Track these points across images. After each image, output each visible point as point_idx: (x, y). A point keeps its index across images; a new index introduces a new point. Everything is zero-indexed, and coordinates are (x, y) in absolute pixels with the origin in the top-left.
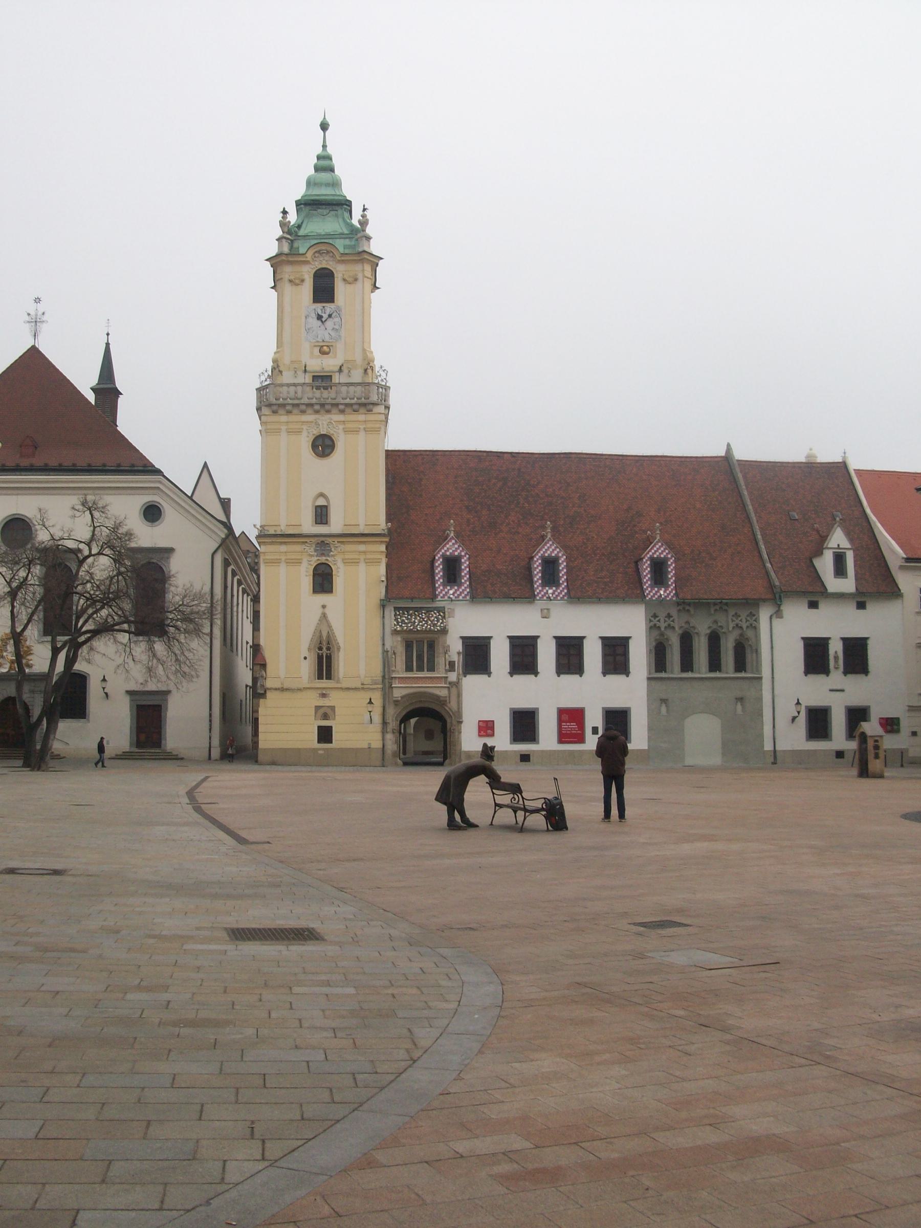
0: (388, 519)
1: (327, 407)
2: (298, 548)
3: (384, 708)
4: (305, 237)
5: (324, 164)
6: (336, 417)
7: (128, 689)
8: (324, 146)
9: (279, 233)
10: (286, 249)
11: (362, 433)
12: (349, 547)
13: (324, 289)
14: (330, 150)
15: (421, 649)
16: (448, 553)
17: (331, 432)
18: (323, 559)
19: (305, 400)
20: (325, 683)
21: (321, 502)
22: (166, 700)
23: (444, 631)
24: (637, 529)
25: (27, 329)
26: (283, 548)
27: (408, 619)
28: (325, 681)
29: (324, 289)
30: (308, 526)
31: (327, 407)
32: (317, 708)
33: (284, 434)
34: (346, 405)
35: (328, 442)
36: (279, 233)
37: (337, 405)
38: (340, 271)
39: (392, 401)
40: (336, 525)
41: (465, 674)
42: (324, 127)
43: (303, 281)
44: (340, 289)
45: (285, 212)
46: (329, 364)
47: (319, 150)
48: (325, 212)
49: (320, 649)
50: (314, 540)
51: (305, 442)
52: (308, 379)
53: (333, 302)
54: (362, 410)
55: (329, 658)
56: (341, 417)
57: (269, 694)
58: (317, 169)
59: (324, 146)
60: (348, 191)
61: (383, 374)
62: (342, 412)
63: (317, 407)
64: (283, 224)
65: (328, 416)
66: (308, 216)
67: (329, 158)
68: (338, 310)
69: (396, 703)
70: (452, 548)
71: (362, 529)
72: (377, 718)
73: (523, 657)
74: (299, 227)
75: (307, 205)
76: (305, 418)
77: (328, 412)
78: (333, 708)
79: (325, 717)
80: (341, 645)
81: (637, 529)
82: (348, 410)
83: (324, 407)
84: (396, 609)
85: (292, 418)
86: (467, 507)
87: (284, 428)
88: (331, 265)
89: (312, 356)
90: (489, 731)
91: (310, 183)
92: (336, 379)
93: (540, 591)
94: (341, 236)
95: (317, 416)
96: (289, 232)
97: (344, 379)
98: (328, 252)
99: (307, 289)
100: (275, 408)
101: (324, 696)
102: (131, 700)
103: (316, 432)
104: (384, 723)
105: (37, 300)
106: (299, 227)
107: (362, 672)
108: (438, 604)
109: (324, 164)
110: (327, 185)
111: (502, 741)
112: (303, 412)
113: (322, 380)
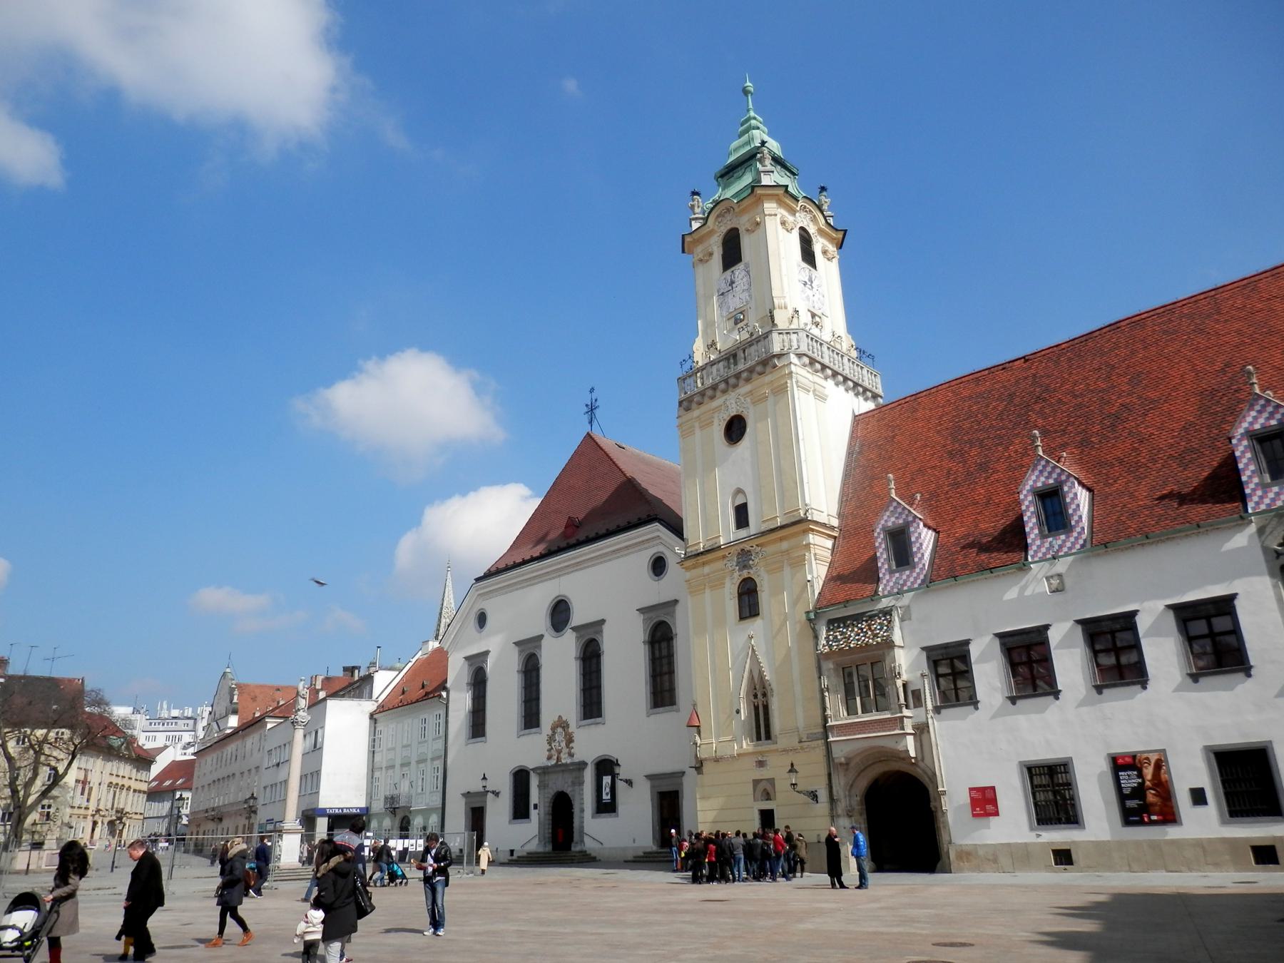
1: (732, 381)
2: (720, 564)
3: (830, 775)
6: (744, 389)
7: (649, 772)
12: (769, 549)
15: (864, 676)
16: (890, 524)
18: (745, 574)
20: (765, 746)
21: (739, 501)
22: (682, 784)
23: (889, 645)
24: (1242, 395)
25: (586, 418)
26: (707, 569)
27: (842, 633)
28: (763, 741)
30: (727, 532)
32: (756, 783)
33: (698, 432)
34: (751, 370)
38: (742, 223)
40: (754, 527)
41: (937, 710)
43: (711, 254)
44: (746, 243)
49: (755, 696)
50: (732, 550)
51: (718, 429)
54: (768, 369)
55: (766, 708)
56: (748, 388)
57: (707, 768)
62: (748, 380)
63: (722, 386)
69: (846, 765)
71: (779, 522)
72: (823, 795)
73: (1028, 661)
76: (716, 403)
77: (735, 386)
78: (771, 781)
79: (768, 796)
80: (774, 686)
81: (1242, 395)
83: (728, 384)
84: (831, 622)
85: (704, 408)
86: (950, 453)
87: (697, 424)
90: (990, 807)
93: (1039, 547)
95: (726, 396)
99: (717, 259)
100: (685, 404)
101: (761, 764)
102: (652, 787)
103: (727, 417)
104: (832, 800)
105: (592, 390)
107: (801, 723)
108: (885, 603)
111: (1014, 821)
112: (712, 398)
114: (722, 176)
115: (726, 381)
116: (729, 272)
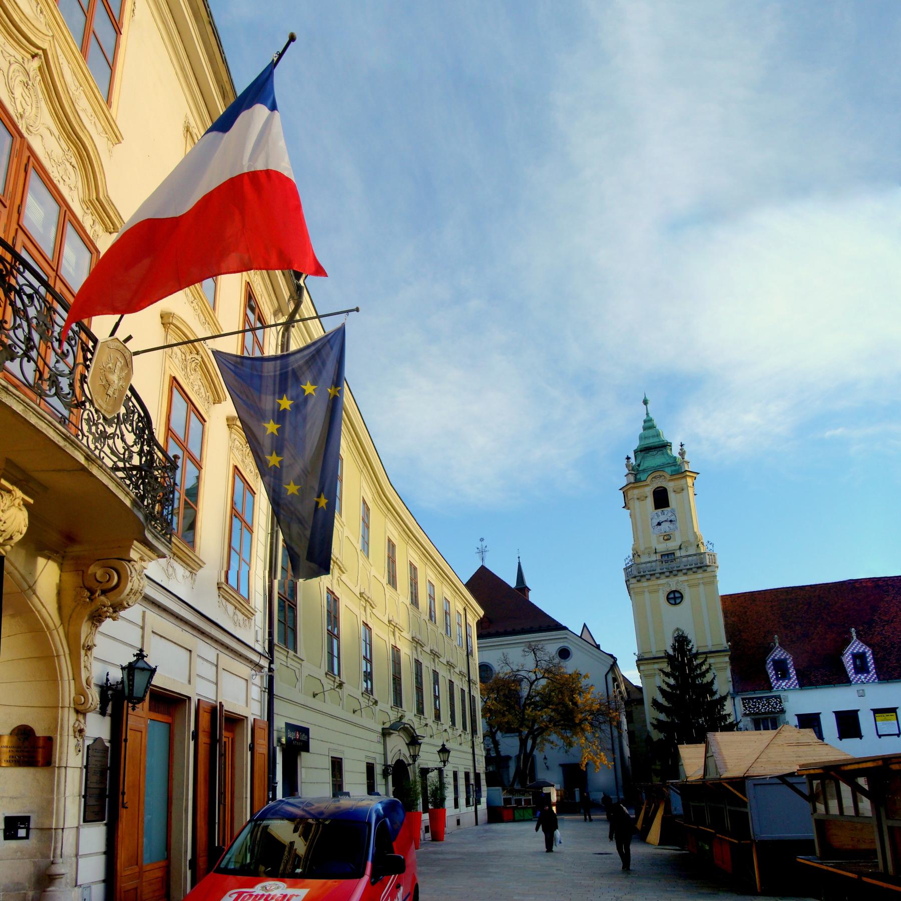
0: (728, 641)
1: (675, 573)
4: (644, 471)
5: (649, 425)
8: (647, 414)
9: (627, 471)
10: (632, 480)
11: (702, 586)
13: (661, 499)
14: (651, 415)
17: (678, 588)
19: (658, 571)
23: (783, 711)
29: (661, 499)
31: (675, 573)
35: (677, 595)
36: (627, 471)
37: (681, 570)
38: (670, 486)
39: (718, 563)
42: (645, 402)
44: (672, 497)
45: (628, 458)
46: (672, 545)
47: (645, 417)
48: (654, 453)
52: (658, 557)
53: (668, 506)
54: (700, 571)
56: (685, 578)
58: (645, 429)
59: (647, 414)
60: (666, 437)
61: (710, 547)
62: (685, 574)
63: (668, 574)
64: (627, 466)
65: (676, 578)
66: (643, 458)
67: (650, 420)
68: (673, 512)
70: (779, 653)
74: (639, 465)
75: (644, 451)
76: (659, 582)
77: (675, 575)
82: (690, 572)
83: (672, 573)
88: (664, 484)
89: (659, 542)
91: (641, 438)
92: (678, 554)
94: (668, 465)
95: (668, 579)
96: (633, 470)
97: (683, 553)
98: (661, 476)
99: (650, 501)
103: (669, 590)
106: (639, 465)
109: (649, 425)
110: (654, 436)
113: (668, 556)
114: (641, 451)
115: (671, 572)
116: (660, 510)
